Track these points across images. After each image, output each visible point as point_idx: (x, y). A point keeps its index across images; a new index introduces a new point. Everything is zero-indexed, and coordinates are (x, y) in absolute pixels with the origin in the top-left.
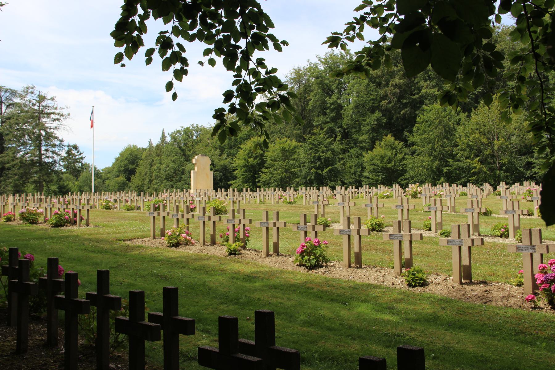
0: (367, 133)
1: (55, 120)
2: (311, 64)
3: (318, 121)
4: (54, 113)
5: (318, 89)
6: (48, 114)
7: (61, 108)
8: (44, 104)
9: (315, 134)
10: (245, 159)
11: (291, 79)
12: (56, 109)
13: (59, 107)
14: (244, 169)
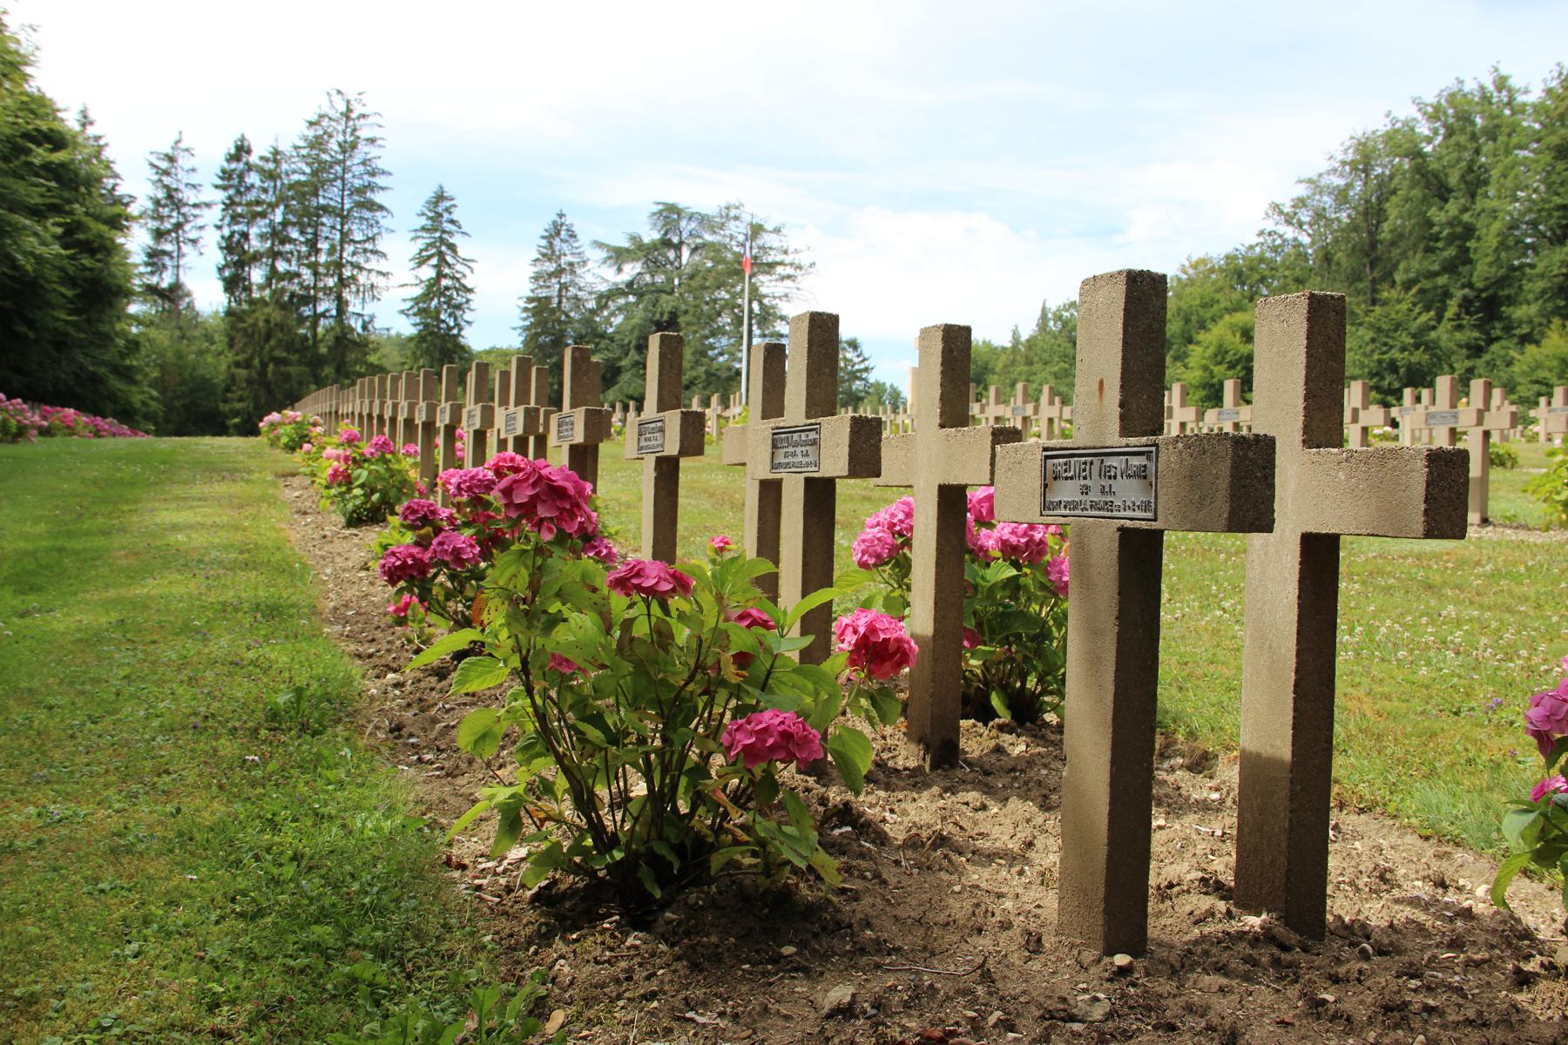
0: (1537, 299)
1: (783, 278)
2: (1394, 121)
3: (1407, 271)
4: (781, 263)
5: (1412, 188)
6: (772, 265)
7: (796, 251)
8: (760, 242)
9: (1385, 303)
10: (1205, 368)
11: (1344, 163)
12: (786, 252)
13: (791, 250)
14: (1203, 393)
